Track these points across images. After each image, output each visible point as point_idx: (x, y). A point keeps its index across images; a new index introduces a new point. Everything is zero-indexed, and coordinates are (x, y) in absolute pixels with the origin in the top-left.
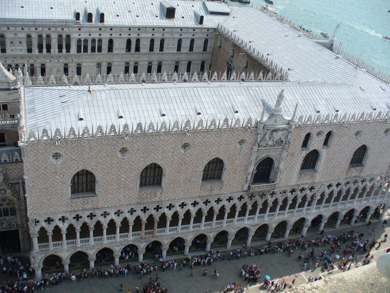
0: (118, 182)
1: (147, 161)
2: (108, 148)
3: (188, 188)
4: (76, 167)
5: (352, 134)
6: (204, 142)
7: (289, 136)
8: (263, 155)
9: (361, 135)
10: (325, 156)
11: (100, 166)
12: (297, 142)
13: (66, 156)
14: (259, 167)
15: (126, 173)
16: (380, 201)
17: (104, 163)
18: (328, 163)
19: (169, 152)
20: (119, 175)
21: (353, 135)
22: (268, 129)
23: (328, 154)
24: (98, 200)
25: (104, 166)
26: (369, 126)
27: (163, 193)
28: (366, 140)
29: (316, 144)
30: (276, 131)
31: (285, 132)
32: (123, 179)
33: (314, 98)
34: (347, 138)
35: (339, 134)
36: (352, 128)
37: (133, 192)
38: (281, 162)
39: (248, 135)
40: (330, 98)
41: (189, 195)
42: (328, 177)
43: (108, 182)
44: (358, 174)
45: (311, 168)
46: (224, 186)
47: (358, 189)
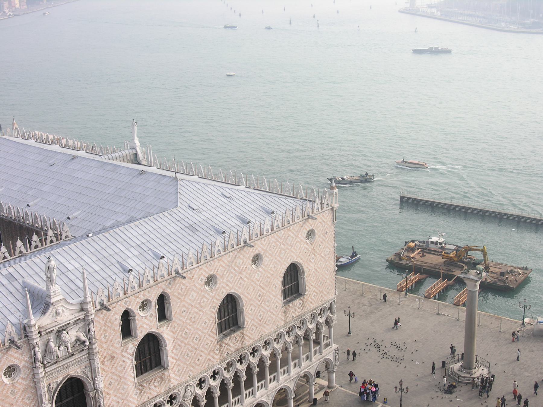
5: (200, 284)
7: (93, 329)
8: (60, 378)
9: (216, 281)
10: (169, 337)
14: (61, 401)
16: (296, 372)
18: (180, 346)
21: (202, 286)
22: (48, 331)
23: (174, 333)
28: (227, 285)
29: (146, 323)
30: (65, 330)
31: (81, 324)
33: (117, 250)
34: (195, 294)
35: (179, 294)
36: (196, 276)
38: (96, 377)
39: (16, 355)
40: (144, 241)
42: (192, 368)
44: (239, 345)
45: (156, 366)
47: (251, 369)
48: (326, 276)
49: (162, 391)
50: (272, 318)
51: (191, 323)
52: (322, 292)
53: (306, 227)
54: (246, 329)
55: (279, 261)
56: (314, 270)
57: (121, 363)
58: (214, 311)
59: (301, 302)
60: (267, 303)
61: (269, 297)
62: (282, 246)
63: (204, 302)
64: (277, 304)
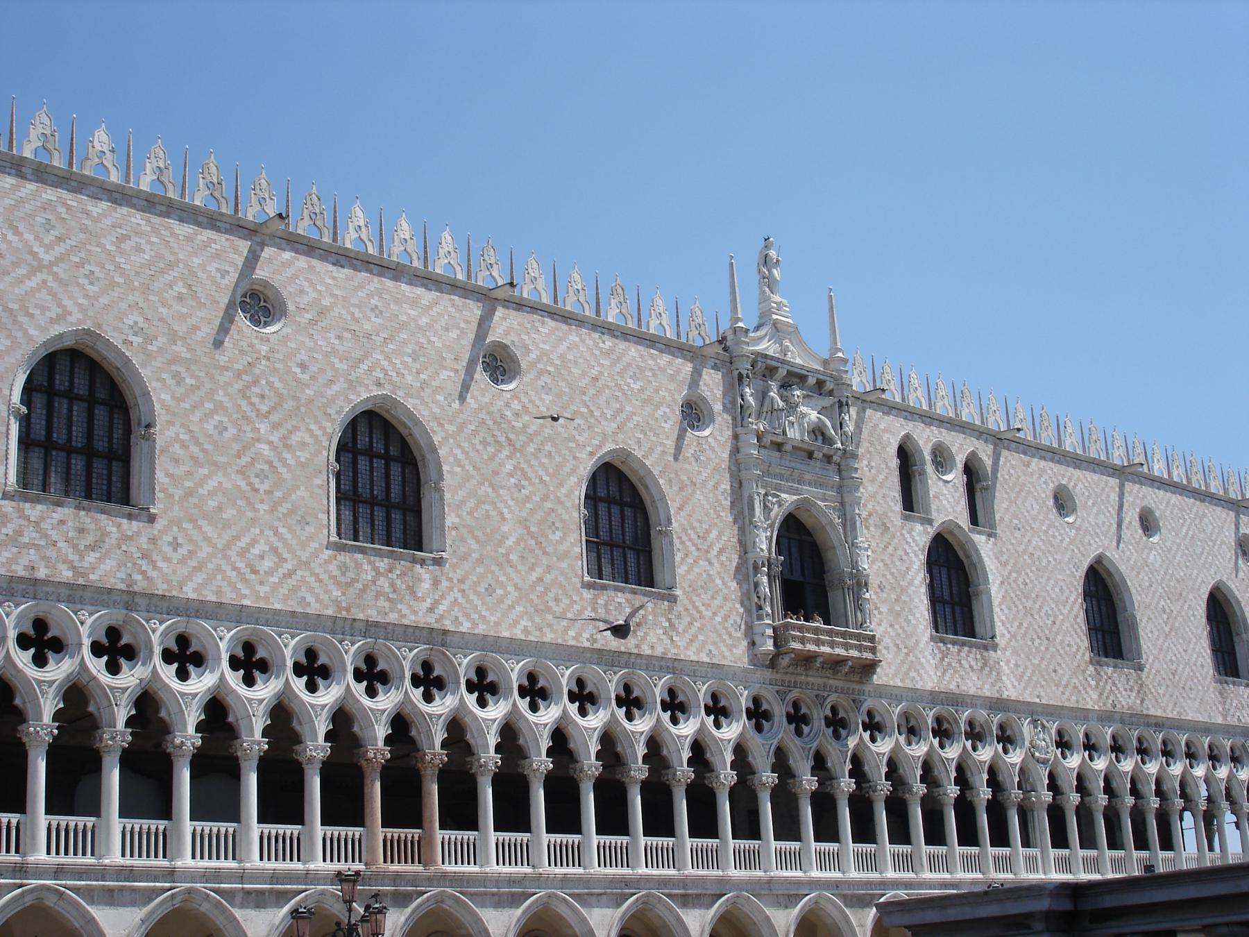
0: (244, 460)
1: (359, 382)
2: (197, 261)
3: (540, 580)
4: (54, 311)
6: (562, 357)
11: (161, 341)
12: (879, 472)
13: (10, 237)
15: (275, 418)
17: (181, 329)
19: (444, 367)
20: (246, 418)
24: (153, 540)
25: (180, 348)
27: (445, 584)
32: (264, 449)
34: (1036, 507)
37: (310, 538)
41: (550, 626)
43: (198, 444)
46: (679, 617)
49: (987, 692)
57: (900, 552)
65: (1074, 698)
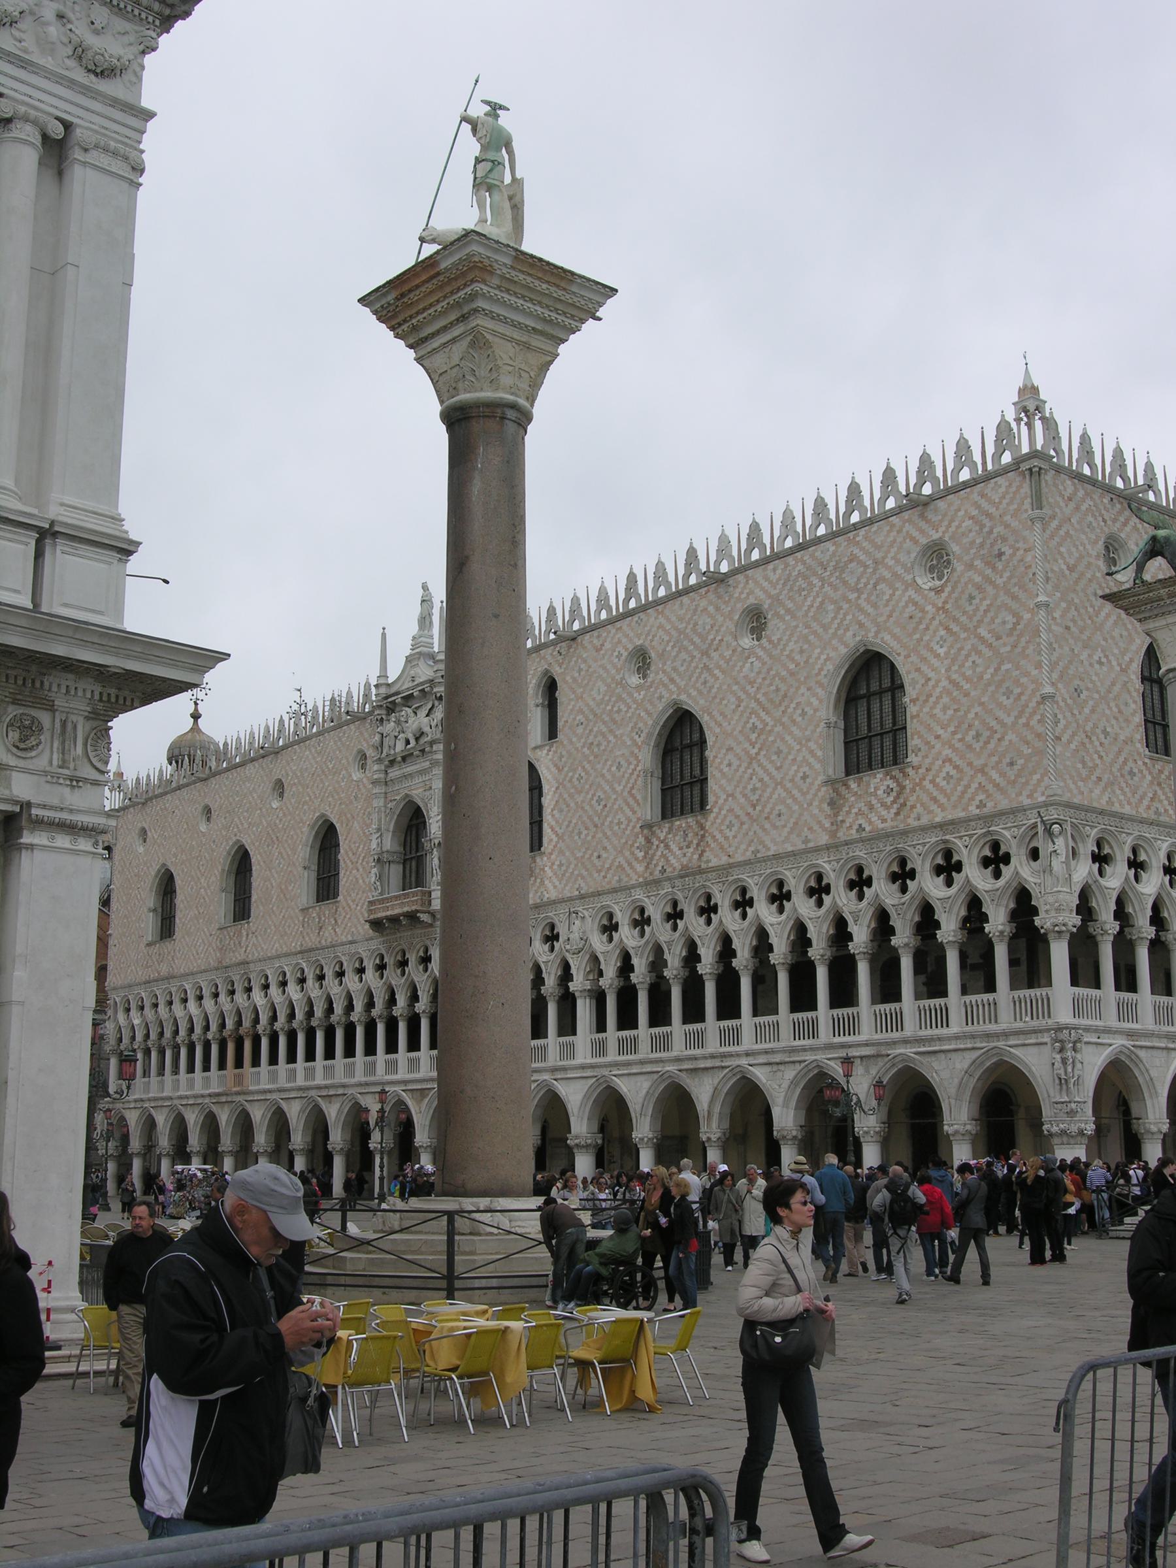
5: (615, 666)
10: (550, 777)
18: (568, 806)
23: (556, 765)
26: (668, 620)
28: (672, 680)
34: (603, 688)
35: (575, 680)
36: (608, 645)
44: (691, 857)
48: (1001, 714)
50: (788, 807)
51: (592, 758)
52: (982, 770)
53: (915, 534)
54: (713, 815)
55: (815, 633)
56: (944, 683)
58: (639, 741)
59: (893, 785)
60: (774, 757)
61: (783, 739)
62: (827, 588)
63: (619, 711)
64: (806, 769)
65: (616, 878)
